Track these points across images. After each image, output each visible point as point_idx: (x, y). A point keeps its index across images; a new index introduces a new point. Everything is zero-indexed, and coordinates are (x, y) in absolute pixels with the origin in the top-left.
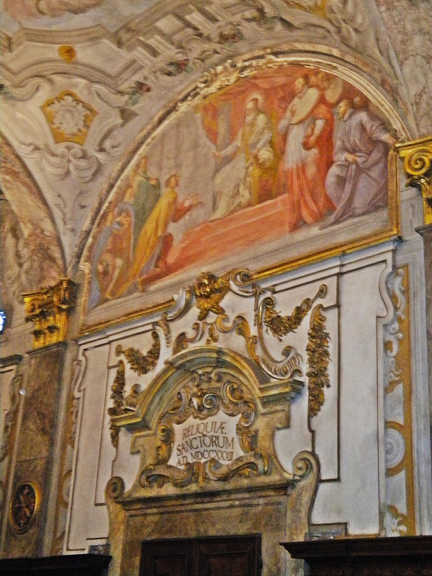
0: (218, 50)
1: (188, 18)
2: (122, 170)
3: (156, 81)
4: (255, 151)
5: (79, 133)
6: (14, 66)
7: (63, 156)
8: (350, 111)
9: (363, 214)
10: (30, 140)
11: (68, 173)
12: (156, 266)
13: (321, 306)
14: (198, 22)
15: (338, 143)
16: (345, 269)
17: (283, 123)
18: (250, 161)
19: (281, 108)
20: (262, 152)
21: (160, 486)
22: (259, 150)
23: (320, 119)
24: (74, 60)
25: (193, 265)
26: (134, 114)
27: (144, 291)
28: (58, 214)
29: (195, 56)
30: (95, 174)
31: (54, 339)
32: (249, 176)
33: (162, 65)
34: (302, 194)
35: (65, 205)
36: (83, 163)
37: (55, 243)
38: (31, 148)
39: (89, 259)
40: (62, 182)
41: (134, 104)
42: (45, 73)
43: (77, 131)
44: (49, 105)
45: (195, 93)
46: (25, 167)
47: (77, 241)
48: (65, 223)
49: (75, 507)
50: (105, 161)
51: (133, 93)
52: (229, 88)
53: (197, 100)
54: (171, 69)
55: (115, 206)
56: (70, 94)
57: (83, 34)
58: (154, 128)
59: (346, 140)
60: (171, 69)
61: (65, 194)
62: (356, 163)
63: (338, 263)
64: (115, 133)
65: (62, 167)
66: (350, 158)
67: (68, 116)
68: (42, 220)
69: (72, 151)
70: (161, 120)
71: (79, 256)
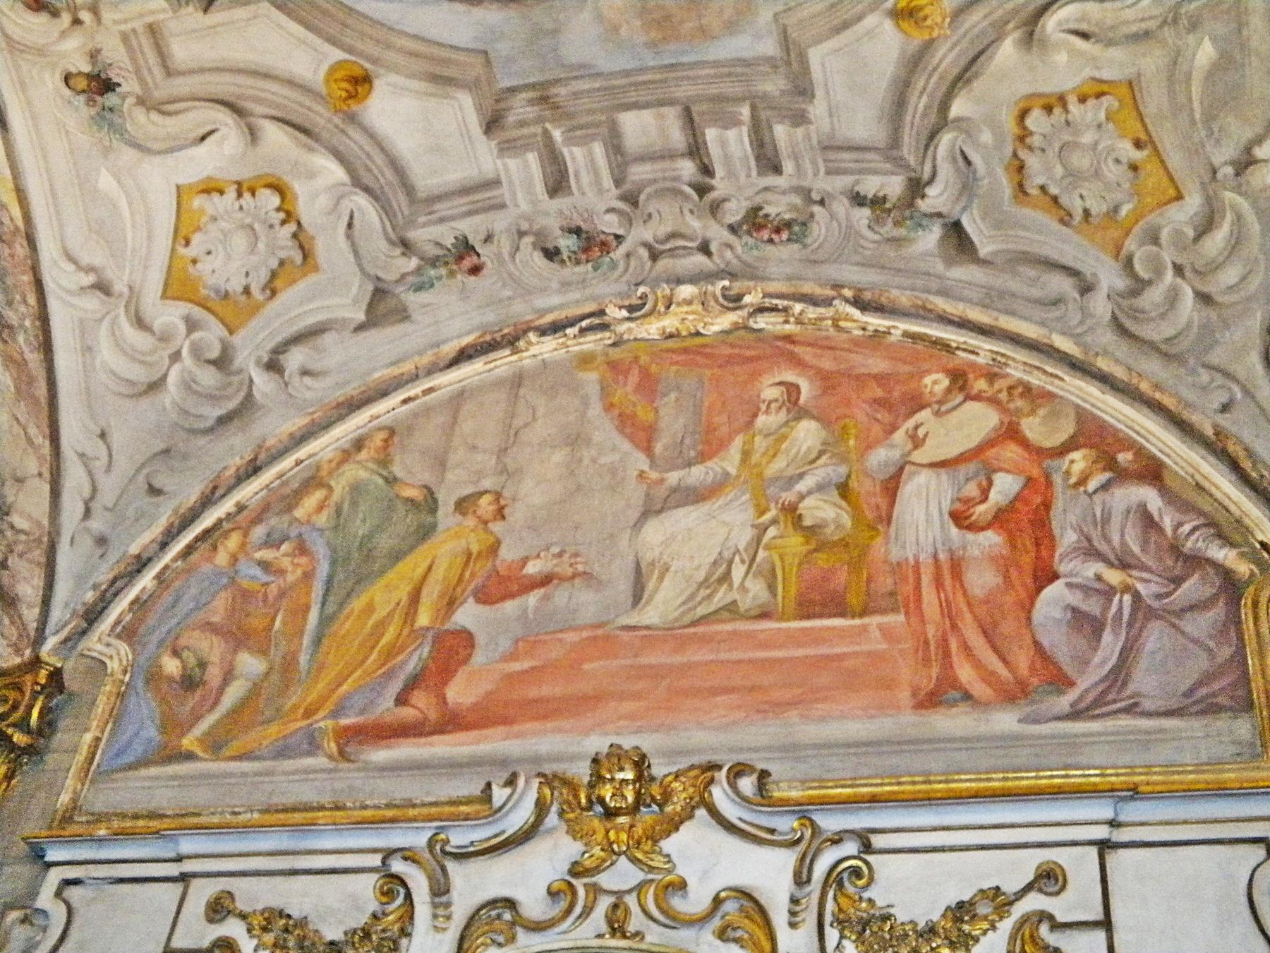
0: (713, 248)
1: (711, 134)
2: (300, 439)
3: (507, 257)
4: (789, 497)
5: (243, 298)
6: (181, 52)
7: (164, 338)
11: (156, 386)
12: (401, 700)
14: (727, 158)
17: (882, 457)
18: (767, 517)
19: (878, 420)
20: (808, 502)
22: (802, 497)
23: (1008, 471)
24: (355, 107)
25: (549, 725)
26: (402, 314)
27: (343, 755)
29: (648, 236)
30: (223, 421)
33: (553, 224)
34: (954, 626)
35: (109, 468)
36: (208, 378)
37: (38, 555)
38: (90, 279)
39: (128, 633)
40: (129, 404)
41: (419, 288)
42: (249, 105)
43: (240, 289)
44: (207, 191)
45: (597, 322)
46: (43, 318)
47: (103, 576)
48: (87, 513)
50: (265, 395)
51: (434, 262)
53: (591, 343)
54: (567, 243)
55: (257, 520)
56: (279, 188)
57: (416, 55)
58: (432, 370)
60: (567, 243)
61: (116, 438)
62: (1127, 589)
63: (1108, 813)
64: (328, 339)
67: (240, 241)
68: (20, 481)
69: (196, 335)
70: (463, 356)
71: (92, 616)
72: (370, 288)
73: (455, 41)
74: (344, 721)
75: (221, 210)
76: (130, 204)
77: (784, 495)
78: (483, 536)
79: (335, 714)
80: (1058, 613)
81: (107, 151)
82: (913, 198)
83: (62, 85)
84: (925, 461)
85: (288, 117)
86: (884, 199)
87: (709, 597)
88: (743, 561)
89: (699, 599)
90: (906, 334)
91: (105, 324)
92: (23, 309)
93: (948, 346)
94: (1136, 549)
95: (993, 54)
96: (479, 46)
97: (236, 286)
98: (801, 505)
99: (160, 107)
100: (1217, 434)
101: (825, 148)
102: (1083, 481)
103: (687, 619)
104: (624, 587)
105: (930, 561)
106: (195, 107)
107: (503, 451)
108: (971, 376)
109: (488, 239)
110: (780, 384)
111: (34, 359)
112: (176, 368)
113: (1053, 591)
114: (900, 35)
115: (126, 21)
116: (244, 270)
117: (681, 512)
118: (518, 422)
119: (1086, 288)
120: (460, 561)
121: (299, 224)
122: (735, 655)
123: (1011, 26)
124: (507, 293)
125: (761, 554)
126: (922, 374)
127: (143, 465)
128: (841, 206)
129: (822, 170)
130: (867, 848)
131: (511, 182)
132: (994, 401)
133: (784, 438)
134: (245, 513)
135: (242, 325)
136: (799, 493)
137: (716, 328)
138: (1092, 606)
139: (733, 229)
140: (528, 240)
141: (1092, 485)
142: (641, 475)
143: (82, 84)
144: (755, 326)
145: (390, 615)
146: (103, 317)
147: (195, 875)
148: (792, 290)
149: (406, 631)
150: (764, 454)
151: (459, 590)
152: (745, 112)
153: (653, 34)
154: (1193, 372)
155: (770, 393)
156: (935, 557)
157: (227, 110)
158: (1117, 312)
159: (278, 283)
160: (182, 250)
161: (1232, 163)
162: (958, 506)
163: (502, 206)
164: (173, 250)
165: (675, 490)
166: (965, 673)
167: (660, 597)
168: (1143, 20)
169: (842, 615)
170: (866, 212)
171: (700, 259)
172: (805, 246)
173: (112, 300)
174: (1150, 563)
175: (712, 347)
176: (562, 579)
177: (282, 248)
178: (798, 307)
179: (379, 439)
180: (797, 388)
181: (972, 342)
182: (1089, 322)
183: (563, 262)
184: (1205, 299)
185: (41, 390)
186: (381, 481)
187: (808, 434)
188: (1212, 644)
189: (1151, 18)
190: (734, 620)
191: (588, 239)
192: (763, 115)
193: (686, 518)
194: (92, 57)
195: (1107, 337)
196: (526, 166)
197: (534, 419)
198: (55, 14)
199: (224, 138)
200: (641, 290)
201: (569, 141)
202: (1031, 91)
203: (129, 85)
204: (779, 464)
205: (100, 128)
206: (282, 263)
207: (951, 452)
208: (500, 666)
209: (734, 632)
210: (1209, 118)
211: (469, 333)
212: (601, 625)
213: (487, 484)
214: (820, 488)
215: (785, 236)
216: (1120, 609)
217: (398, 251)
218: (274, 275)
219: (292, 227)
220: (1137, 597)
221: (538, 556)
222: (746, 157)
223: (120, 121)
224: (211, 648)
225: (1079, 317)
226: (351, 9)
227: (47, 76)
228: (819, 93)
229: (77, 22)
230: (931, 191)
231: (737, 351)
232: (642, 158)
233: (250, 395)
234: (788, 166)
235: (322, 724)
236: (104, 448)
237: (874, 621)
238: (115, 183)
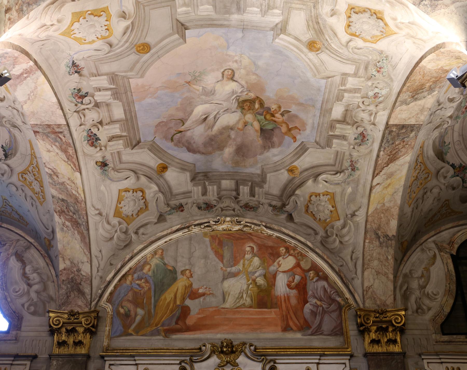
0: (236, 210)
8: (317, 278)
10: (99, 207)
16: (321, 362)
20: (258, 279)
22: (256, 278)
23: (298, 275)
25: (209, 331)
28: (95, 262)
34: (289, 312)
38: (97, 212)
41: (169, 214)
43: (131, 215)
51: (173, 209)
52: (230, 232)
59: (315, 292)
60: (203, 206)
62: (321, 306)
67: (132, 203)
72: (159, 214)
73: (188, 161)
74: (165, 328)
75: (128, 196)
76: (108, 193)
77: (253, 277)
78: (188, 281)
79: (163, 325)
80: (308, 311)
81: (103, 180)
82: (283, 207)
83: (95, 164)
84: (281, 271)
85: (147, 175)
86: (276, 206)
87: (239, 302)
88: (245, 293)
89: (237, 302)
90: (277, 237)
91: (101, 223)
92: (83, 220)
93: (285, 241)
94: (323, 297)
95: (306, 183)
96: (194, 163)
97: (130, 214)
98: (256, 280)
99: (117, 171)
100: (339, 271)
101: (266, 194)
102: (312, 279)
103: (235, 307)
104: (221, 297)
105: (283, 296)
106: (125, 171)
107: (190, 258)
108: (290, 249)
109: (186, 204)
110: (249, 246)
111: (85, 232)
112: (116, 234)
113: (308, 305)
114: (288, 175)
115: (113, 150)
116: (132, 210)
117: (231, 279)
118: (192, 251)
120: (184, 288)
121: (146, 200)
122: (246, 316)
123: (312, 177)
124: (188, 216)
125: (249, 292)
126: (280, 247)
127: (109, 259)
128: (266, 206)
129: (264, 198)
130: (275, 363)
131: (194, 192)
132: (294, 256)
133: (252, 261)
134: (132, 270)
135: (131, 223)
136: (256, 276)
137: (235, 229)
138: (315, 310)
139: (241, 207)
140: (195, 205)
141: (314, 280)
142: (221, 268)
143: (99, 164)
144: (244, 230)
145: (170, 301)
146: (100, 222)
147: (139, 364)
148: (252, 222)
149: (175, 305)
150: (248, 265)
151: (185, 295)
152: (250, 184)
153: (234, 165)
154: (336, 257)
155: (248, 249)
156: (285, 296)
157: (133, 172)
158: (322, 240)
159: (139, 213)
160: (119, 205)
161: (351, 214)
162: (288, 283)
163: (191, 197)
164: (117, 205)
165: (229, 273)
166: (291, 324)
167: (229, 301)
168: (338, 181)
169: (266, 308)
170: (272, 208)
171: (232, 212)
172: (256, 212)
173: (102, 217)
174: (325, 300)
175: (234, 234)
176: (207, 295)
177: (141, 205)
178: (253, 226)
179: (160, 251)
180: (253, 248)
181: (290, 240)
182: (315, 241)
183: (202, 210)
185: (87, 241)
186: (162, 264)
187: (256, 261)
188: (336, 320)
189: (340, 180)
190: (245, 308)
191: (208, 205)
192: (254, 185)
194: (103, 158)
195: (319, 245)
196: (198, 189)
197: (196, 250)
198: (96, 147)
199: (131, 179)
200: (218, 218)
201: (209, 185)
202: (314, 191)
203: (111, 165)
204: (251, 269)
205: (103, 175)
206: (141, 209)
207: (286, 269)
208: (197, 316)
209: (245, 311)
210: (348, 204)
211: (179, 225)
212: (217, 307)
213: (187, 267)
214: (260, 276)
215: (252, 210)
216: (320, 311)
217: (166, 206)
218: (139, 211)
219: (144, 200)
220: (323, 308)
221: (201, 288)
222: (248, 193)
223: (107, 173)
224: (131, 306)
225: (313, 239)
226: (166, 152)
227: (92, 162)
228: (267, 183)
229: (101, 149)
230: (287, 207)
231: (240, 236)
232: (225, 190)
233: (131, 240)
234: (257, 196)
235: (160, 328)
236: (100, 254)
237: (273, 310)
238: (105, 188)
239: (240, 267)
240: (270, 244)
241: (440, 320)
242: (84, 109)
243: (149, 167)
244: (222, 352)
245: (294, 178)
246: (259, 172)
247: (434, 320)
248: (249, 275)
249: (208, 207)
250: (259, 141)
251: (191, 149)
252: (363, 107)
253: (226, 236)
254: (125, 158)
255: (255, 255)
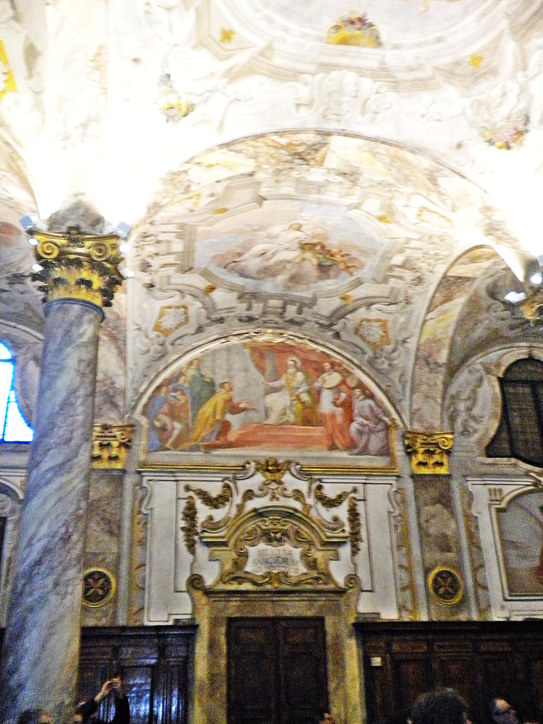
4: (297, 393)
9: (374, 455)
13: (354, 498)
15: (356, 411)
21: (240, 583)
31: (119, 466)
32: (293, 407)
49: (153, 591)
65: (147, 346)
66: (365, 422)
110: (292, 360)
119: (364, 353)
126: (325, 362)
132: (339, 372)
155: (291, 363)
184: (390, 365)
187: (300, 376)
193: (274, 396)
239: (282, 382)
240: (314, 358)
241: (486, 442)
242: (143, 245)
243: (198, 288)
244: (268, 470)
245: (346, 305)
246: (310, 296)
247: (479, 442)
248: (293, 390)
249: (251, 319)
250: (315, 273)
251: (243, 274)
252: (423, 260)
253: (267, 348)
254: (174, 280)
255: (298, 370)
